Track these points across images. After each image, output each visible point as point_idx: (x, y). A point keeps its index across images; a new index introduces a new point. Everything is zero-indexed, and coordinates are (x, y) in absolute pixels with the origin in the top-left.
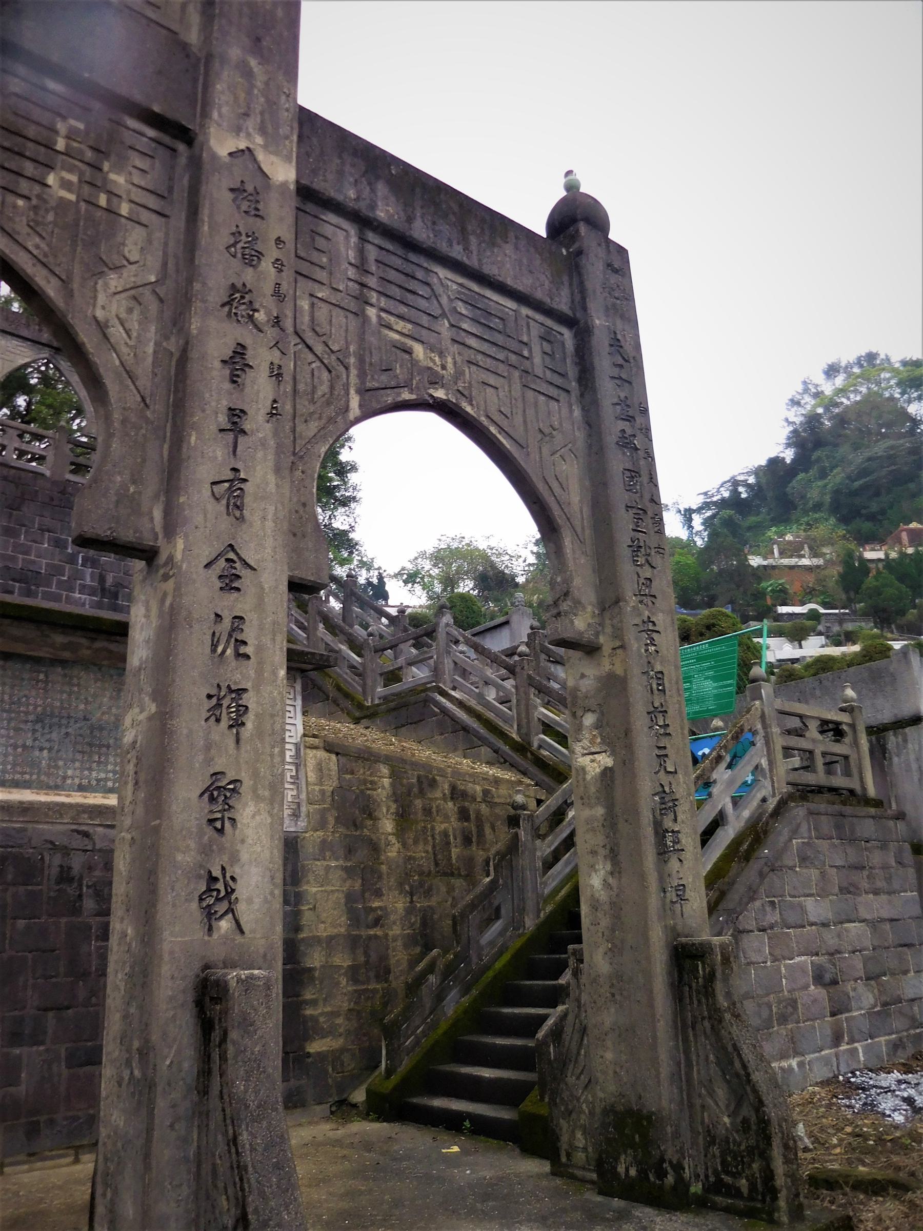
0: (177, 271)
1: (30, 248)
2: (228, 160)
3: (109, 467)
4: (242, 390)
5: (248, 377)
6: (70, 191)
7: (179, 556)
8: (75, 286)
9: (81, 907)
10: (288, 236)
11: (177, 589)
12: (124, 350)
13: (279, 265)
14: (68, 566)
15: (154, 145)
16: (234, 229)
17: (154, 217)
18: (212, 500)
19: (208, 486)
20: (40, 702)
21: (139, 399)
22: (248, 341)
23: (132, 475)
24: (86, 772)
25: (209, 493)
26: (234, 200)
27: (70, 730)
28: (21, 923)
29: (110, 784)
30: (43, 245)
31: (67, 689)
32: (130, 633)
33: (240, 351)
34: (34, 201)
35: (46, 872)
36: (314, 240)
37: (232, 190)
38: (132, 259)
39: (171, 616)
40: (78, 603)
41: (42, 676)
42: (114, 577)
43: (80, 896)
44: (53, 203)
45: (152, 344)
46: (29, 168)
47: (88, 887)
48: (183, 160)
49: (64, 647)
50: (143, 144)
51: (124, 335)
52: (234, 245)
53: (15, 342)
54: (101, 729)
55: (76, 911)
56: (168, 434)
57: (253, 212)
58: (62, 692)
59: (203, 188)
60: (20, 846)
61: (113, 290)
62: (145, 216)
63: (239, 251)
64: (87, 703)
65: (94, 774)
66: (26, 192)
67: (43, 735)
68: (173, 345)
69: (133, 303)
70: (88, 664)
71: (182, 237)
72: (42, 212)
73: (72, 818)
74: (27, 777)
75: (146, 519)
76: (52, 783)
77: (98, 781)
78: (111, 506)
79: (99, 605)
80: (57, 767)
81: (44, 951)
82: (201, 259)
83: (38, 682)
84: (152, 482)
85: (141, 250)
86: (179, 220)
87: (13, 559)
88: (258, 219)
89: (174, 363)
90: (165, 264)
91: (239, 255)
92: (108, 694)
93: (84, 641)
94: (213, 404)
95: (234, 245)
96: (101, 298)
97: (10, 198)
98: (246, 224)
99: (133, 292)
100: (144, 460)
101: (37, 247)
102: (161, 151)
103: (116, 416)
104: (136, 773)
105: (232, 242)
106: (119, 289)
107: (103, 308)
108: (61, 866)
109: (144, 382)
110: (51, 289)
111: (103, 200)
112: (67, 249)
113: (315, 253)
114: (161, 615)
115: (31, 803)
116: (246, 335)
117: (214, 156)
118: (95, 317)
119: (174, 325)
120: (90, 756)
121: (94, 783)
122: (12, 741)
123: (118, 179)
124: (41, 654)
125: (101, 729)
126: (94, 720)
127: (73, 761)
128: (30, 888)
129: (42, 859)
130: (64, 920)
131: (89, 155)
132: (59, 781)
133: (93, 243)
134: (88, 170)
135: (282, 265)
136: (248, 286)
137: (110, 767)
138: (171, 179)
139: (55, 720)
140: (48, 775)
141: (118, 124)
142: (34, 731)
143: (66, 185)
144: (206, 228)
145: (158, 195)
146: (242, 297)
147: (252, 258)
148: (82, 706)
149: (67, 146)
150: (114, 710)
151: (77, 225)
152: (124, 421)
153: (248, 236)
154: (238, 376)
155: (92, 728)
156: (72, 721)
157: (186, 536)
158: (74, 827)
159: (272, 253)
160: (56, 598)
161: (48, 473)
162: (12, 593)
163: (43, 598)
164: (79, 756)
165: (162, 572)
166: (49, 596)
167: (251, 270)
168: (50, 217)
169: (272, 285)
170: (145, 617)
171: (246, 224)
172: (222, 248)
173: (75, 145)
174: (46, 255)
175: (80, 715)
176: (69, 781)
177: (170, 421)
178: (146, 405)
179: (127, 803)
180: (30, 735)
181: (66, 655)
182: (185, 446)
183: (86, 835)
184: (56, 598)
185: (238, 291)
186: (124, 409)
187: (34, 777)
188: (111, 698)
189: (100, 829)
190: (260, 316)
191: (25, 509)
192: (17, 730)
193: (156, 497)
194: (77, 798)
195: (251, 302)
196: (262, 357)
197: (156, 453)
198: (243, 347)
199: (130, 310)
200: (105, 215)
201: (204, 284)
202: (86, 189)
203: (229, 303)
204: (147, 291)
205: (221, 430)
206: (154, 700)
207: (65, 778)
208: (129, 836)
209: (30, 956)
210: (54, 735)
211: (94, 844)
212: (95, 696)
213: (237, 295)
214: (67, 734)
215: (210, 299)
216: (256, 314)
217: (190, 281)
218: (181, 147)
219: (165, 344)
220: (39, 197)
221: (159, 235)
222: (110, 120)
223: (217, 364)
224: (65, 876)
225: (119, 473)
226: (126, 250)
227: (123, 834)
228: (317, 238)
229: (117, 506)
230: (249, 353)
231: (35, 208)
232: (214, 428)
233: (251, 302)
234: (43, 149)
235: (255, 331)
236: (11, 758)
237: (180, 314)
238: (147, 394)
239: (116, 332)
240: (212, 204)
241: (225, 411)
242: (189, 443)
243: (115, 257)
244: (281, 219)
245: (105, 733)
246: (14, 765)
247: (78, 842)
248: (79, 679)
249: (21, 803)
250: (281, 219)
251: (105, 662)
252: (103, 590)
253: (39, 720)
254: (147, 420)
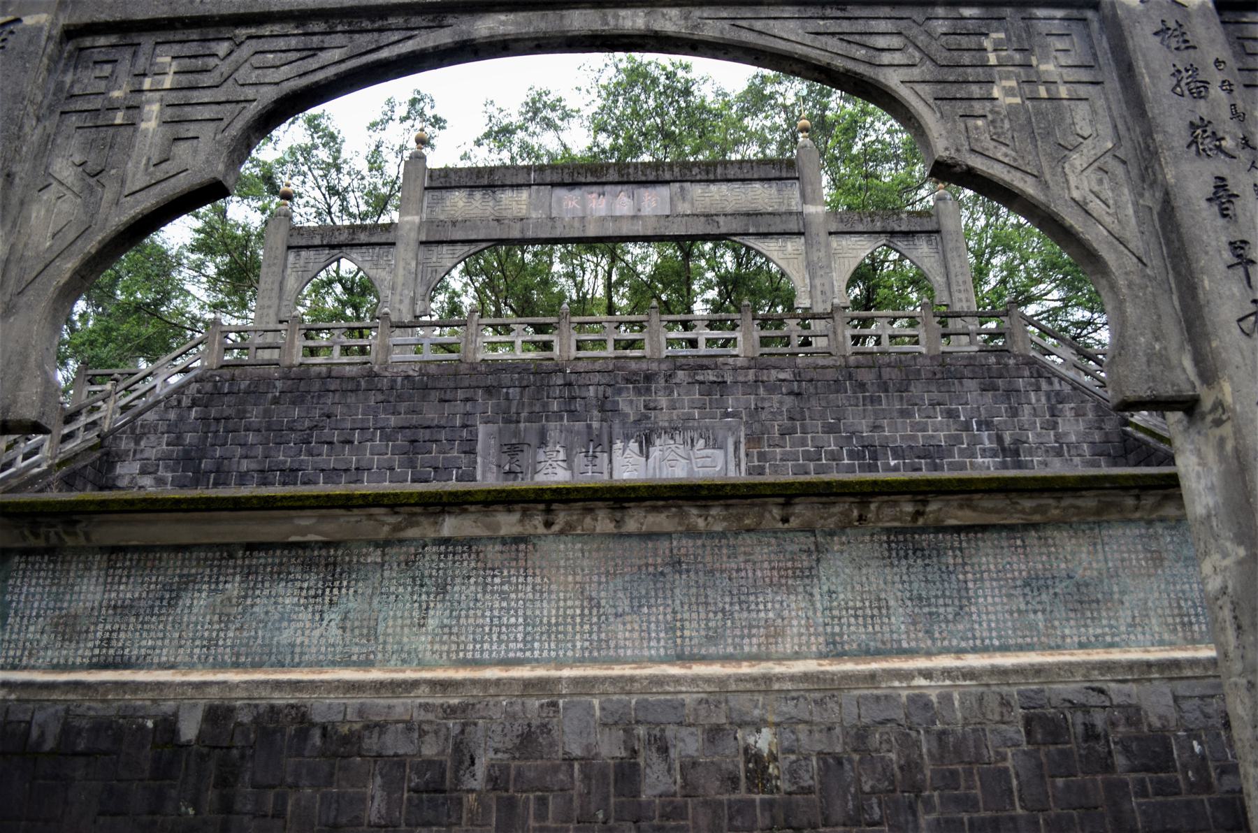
0: (1128, 129)
1: (1001, 158)
2: (1142, 7)
3: (1130, 331)
4: (1236, 221)
5: (1238, 207)
6: (1014, 96)
7: (1229, 399)
8: (1048, 177)
9: (1113, 763)
10: (1224, 53)
11: (1238, 432)
12: (1108, 220)
13: (1227, 86)
14: (964, 434)
15: (1066, 23)
16: (1173, 70)
17: (1090, 87)
18: (1244, 337)
19: (1235, 324)
20: (1023, 567)
21: (1135, 260)
22: (1225, 172)
23: (1154, 333)
24: (1083, 630)
25: (1239, 331)
26: (1162, 43)
27: (1057, 590)
28: (1060, 782)
29: (1108, 639)
30: (1010, 152)
31: (1044, 550)
32: (1182, 483)
33: (1221, 182)
34: (990, 117)
35: (1072, 730)
36: (1243, 46)
37: (1156, 34)
38: (1086, 135)
39: (1238, 458)
40: (981, 467)
41: (1019, 542)
42: (1011, 435)
43: (1110, 752)
44: (1004, 112)
45: (1130, 205)
46: (976, 90)
47: (1115, 743)
48: (1095, 26)
49: (1035, 511)
50: (1056, 26)
51: (1104, 206)
52: (1178, 85)
53: (854, 239)
54: (1087, 585)
55: (1109, 767)
56: (1173, 286)
57: (1183, 46)
58: (1041, 554)
59: (1130, 44)
60: (1042, 707)
61: (1080, 168)
62: (1083, 91)
63: (1185, 88)
64: (1067, 561)
65: (1091, 631)
66: (981, 112)
67: (1033, 597)
68: (1151, 200)
69: (1101, 174)
70: (1059, 524)
71: (1121, 96)
72: (999, 124)
73: (1084, 676)
74: (1028, 640)
75: (1179, 371)
76: (1053, 644)
77: (1096, 636)
78: (1144, 367)
79: (1004, 466)
80: (1054, 628)
81: (1088, 809)
82: (1153, 110)
83: (1016, 547)
84: (1174, 335)
85: (1092, 123)
86: (1113, 82)
87: (914, 438)
88: (1191, 51)
89: (1156, 217)
90: (1115, 127)
91: (1187, 93)
92: (1084, 549)
93: (1051, 501)
94: (1214, 243)
95: (1178, 85)
96: (1073, 180)
97: (971, 122)
98: (1181, 60)
99: (1096, 164)
100: (1159, 317)
101: (1006, 155)
102: (1074, 25)
103: (1122, 282)
104: (1235, 618)
105: (1174, 82)
106: (1085, 165)
107: (1077, 188)
108: (1084, 724)
109: (1136, 243)
110: (1029, 187)
111: (1043, 92)
112: (1030, 147)
113: (1250, 59)
114: (1222, 457)
115: (1041, 665)
116: (1220, 166)
117: (1129, 10)
118: (1073, 199)
119: (1144, 181)
120: (1083, 614)
121: (1093, 639)
122: (1007, 607)
123: (1048, 68)
124: (1014, 521)
125: (1087, 585)
126: (1077, 577)
127: (1068, 620)
128: (1060, 746)
129: (1065, 717)
130: (1099, 777)
131: (1018, 57)
132: (1059, 641)
133: (1049, 133)
134: (1021, 70)
135: (1230, 85)
136: (1206, 119)
137: (1104, 622)
138: (1092, 47)
139: (1041, 582)
140: (1048, 636)
141: (1030, 19)
142: (1025, 595)
143: (1009, 92)
144: (1147, 79)
145: (1086, 67)
146: (1205, 131)
147: (1199, 90)
148: (1063, 566)
149: (998, 58)
150: (1094, 565)
151: (1030, 122)
152: (1130, 286)
153: (1187, 71)
154: (1227, 209)
155: (1078, 585)
156: (1057, 581)
157: (1231, 378)
158: (1088, 684)
159: (1216, 78)
160: (962, 467)
161: (924, 350)
162: (920, 469)
163: (949, 469)
164: (1072, 615)
165: (1209, 418)
166: (953, 466)
167: (1202, 102)
168: (1007, 125)
169: (1227, 108)
170: (1199, 464)
171: (1181, 60)
172: (1168, 92)
173: (1004, 53)
174: (1015, 160)
175: (1064, 574)
176: (1068, 640)
177: (1171, 272)
178: (1145, 265)
179: (1231, 648)
180: (1021, 599)
181: (1037, 518)
182: (1200, 292)
183: (1101, 691)
184: (962, 467)
185: (1198, 127)
186: (1126, 273)
187: (1035, 639)
188: (1089, 553)
189: (1113, 685)
190: (1228, 144)
191: (912, 388)
192: (1009, 596)
193: (1182, 348)
194: (1080, 656)
195: (1214, 133)
196: (1241, 182)
197: (1170, 306)
198: (1222, 179)
199: (1100, 182)
200: (1048, 104)
201: (1165, 132)
202: (1026, 88)
203: (1194, 142)
204: (1108, 158)
205: (1229, 267)
206: (1240, 543)
207: (1064, 637)
208: (1244, 681)
209: (1075, 813)
210: (1044, 597)
211: (1111, 699)
212: (1073, 553)
213: (1199, 131)
214: (1056, 594)
215: (1175, 144)
216: (1223, 143)
217: (1148, 134)
218: (1089, 14)
219: (1141, 202)
220: (992, 111)
221: (1100, 103)
222: (1023, 19)
223: (1204, 204)
224: (1091, 733)
225: (1142, 334)
226: (1078, 128)
227: (1233, 679)
228: (1246, 43)
229: (1149, 366)
230: (1230, 183)
231: (993, 122)
232: (1222, 267)
233: (1214, 133)
234: (980, 70)
235: (1227, 159)
236: (1010, 624)
237: (1146, 168)
238: (1141, 253)
239: (1095, 206)
240: (1144, 56)
241: (1227, 247)
242: (1204, 288)
243: (1071, 138)
244: (1213, 41)
245: (1091, 589)
246: (1015, 630)
247: (1095, 699)
248: (1054, 539)
249: (1032, 665)
250: (1213, 41)
251: (1075, 519)
252: (1004, 450)
253: (1026, 584)
254: (1150, 278)
